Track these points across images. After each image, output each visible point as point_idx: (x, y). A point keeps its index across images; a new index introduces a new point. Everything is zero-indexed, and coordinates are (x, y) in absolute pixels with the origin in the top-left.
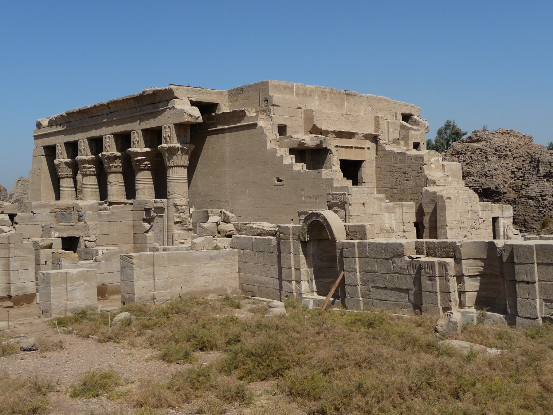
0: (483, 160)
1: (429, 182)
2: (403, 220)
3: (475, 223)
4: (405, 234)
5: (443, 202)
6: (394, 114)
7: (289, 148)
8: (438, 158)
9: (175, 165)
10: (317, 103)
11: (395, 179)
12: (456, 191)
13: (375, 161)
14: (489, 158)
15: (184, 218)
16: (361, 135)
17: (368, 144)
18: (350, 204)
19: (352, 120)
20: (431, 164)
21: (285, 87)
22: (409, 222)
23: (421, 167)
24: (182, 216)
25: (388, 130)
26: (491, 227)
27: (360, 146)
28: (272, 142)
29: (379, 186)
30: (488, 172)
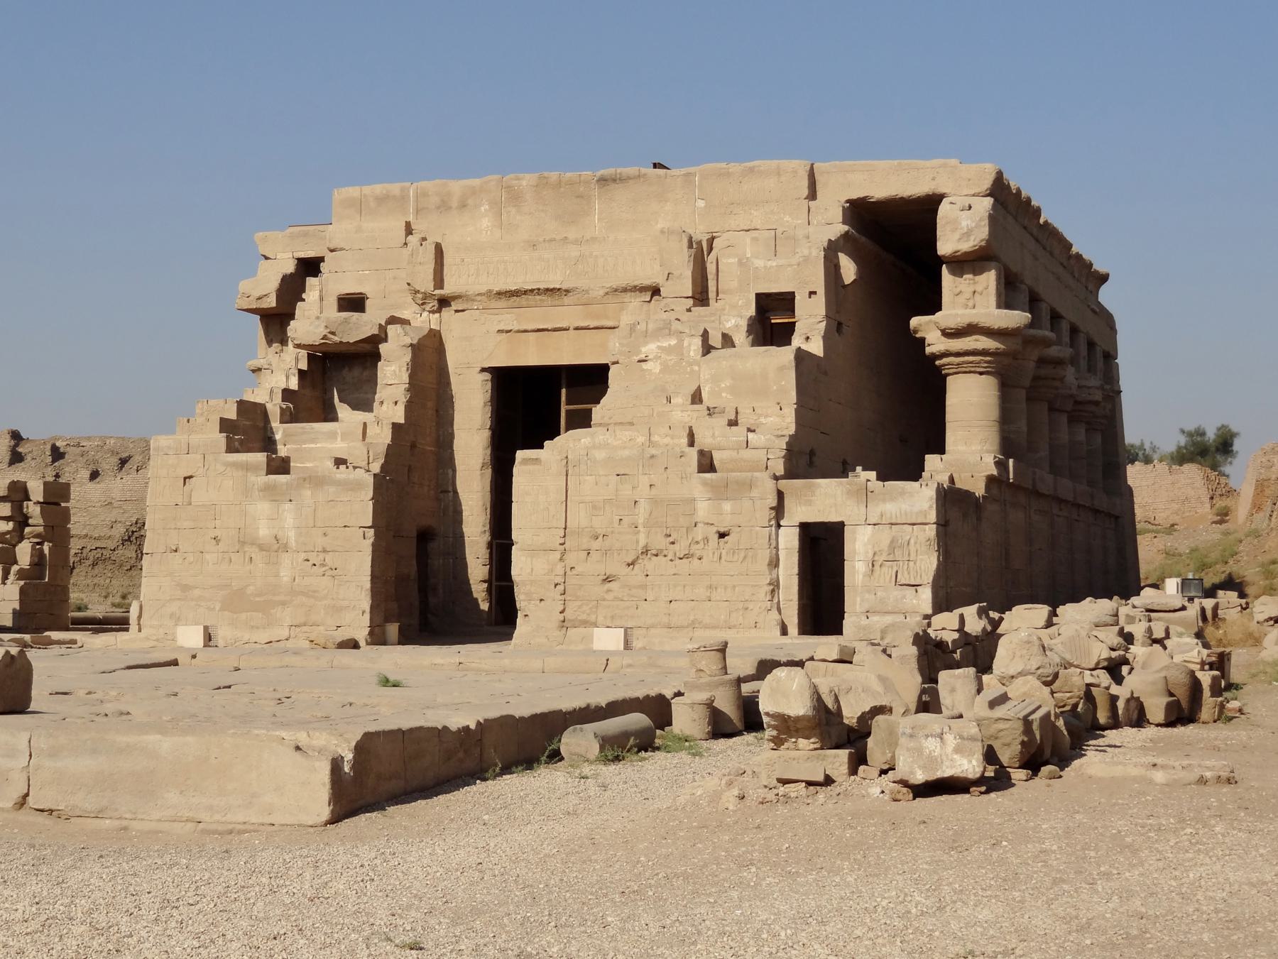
8: (681, 341)
10: (486, 223)
16: (602, 292)
20: (639, 361)
21: (382, 200)
22: (345, 526)
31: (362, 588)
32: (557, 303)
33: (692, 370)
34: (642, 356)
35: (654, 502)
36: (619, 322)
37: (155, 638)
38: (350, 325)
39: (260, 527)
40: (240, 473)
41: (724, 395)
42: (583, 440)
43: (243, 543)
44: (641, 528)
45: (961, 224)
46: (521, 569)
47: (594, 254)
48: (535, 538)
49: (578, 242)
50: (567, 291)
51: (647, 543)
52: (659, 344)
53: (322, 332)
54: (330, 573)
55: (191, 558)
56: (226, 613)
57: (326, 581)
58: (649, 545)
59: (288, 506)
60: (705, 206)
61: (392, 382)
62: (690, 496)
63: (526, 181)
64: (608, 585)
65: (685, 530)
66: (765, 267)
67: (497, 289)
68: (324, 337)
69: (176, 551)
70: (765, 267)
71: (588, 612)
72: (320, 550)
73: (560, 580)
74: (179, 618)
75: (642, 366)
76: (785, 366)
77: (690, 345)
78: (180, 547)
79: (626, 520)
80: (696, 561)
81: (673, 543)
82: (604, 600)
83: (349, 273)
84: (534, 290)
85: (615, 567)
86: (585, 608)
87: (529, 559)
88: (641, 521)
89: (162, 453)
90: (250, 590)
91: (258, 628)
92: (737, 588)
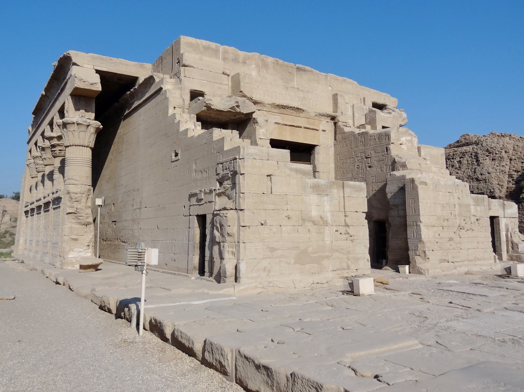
0: (474, 164)
1: (398, 165)
2: (344, 209)
3: (465, 222)
4: (347, 228)
5: (415, 189)
6: (362, 100)
7: (197, 115)
9: (71, 144)
11: (356, 167)
13: (333, 148)
14: (481, 161)
15: (79, 208)
16: (314, 114)
18: (242, 174)
20: (401, 144)
23: (387, 148)
24: (76, 207)
25: (354, 115)
26: (489, 229)
28: (177, 109)
30: (480, 176)
31: (366, 247)
32: (297, 115)
34: (401, 142)
35: (460, 205)
36: (319, 128)
37: (261, 286)
42: (418, 175)
44: (457, 217)
45: (403, 116)
49: (302, 91)
50: (303, 111)
52: (406, 138)
53: (232, 104)
54: (351, 238)
56: (297, 265)
57: (349, 243)
59: (326, 198)
60: (331, 90)
63: (270, 60)
64: (452, 243)
65: (468, 218)
66: (384, 116)
67: (277, 103)
68: (233, 108)
70: (384, 116)
73: (437, 240)
74: (269, 271)
75: (401, 146)
77: (414, 141)
78: (267, 222)
83: (196, 80)
84: (292, 107)
86: (445, 253)
88: (457, 214)
89: (252, 158)
90: (310, 250)
91: (315, 273)
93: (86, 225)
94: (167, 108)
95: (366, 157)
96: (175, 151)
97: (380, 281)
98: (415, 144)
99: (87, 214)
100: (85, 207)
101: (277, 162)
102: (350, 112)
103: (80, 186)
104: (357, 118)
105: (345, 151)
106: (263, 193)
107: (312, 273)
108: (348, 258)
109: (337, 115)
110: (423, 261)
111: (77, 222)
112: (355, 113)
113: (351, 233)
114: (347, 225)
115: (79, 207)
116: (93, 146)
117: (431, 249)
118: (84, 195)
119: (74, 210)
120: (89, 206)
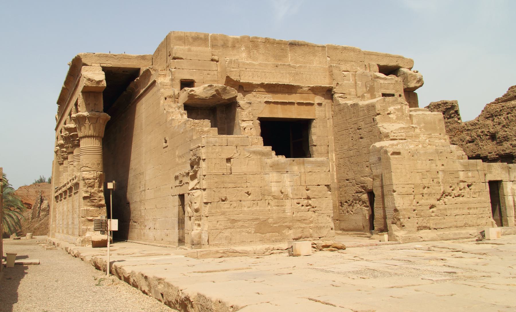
3: (452, 188)
10: (244, 55)
12: (420, 146)
13: (331, 120)
16: (307, 89)
17: (318, 99)
19: (293, 72)
20: (388, 114)
22: (319, 185)
27: (305, 102)
28: (168, 99)
29: (337, 150)
31: (329, 217)
33: (407, 120)
34: (389, 112)
36: (314, 101)
38: (226, 91)
39: (272, 186)
40: (259, 157)
41: (422, 129)
43: (264, 195)
46: (399, 203)
47: (301, 72)
48: (403, 189)
51: (444, 190)
54: (313, 209)
55: (234, 204)
56: (258, 234)
58: (445, 191)
60: (330, 60)
61: (246, 119)
62: (457, 169)
68: (214, 96)
69: (223, 201)
71: (426, 222)
72: (305, 198)
73: (414, 208)
76: (441, 119)
77: (405, 109)
78: (228, 198)
79: (435, 180)
80: (461, 199)
81: (453, 190)
82: (432, 216)
83: (185, 70)
85: (433, 202)
86: (425, 221)
87: (402, 199)
88: (440, 181)
89: (212, 145)
92: (478, 209)
93: (100, 208)
94: (159, 99)
95: (358, 128)
96: (165, 138)
97: (335, 245)
98: (406, 112)
99: (99, 198)
100: (98, 191)
101: (236, 147)
102: (351, 81)
103: (92, 172)
104: (360, 86)
105: (340, 123)
106: (223, 174)
107: (273, 241)
108: (311, 227)
109: (333, 87)
110: (398, 229)
111: (91, 205)
112: (357, 81)
113: (313, 205)
114: (308, 198)
115: (92, 191)
116: (103, 136)
117: (406, 216)
118: (97, 181)
119: (88, 194)
120: (102, 190)
